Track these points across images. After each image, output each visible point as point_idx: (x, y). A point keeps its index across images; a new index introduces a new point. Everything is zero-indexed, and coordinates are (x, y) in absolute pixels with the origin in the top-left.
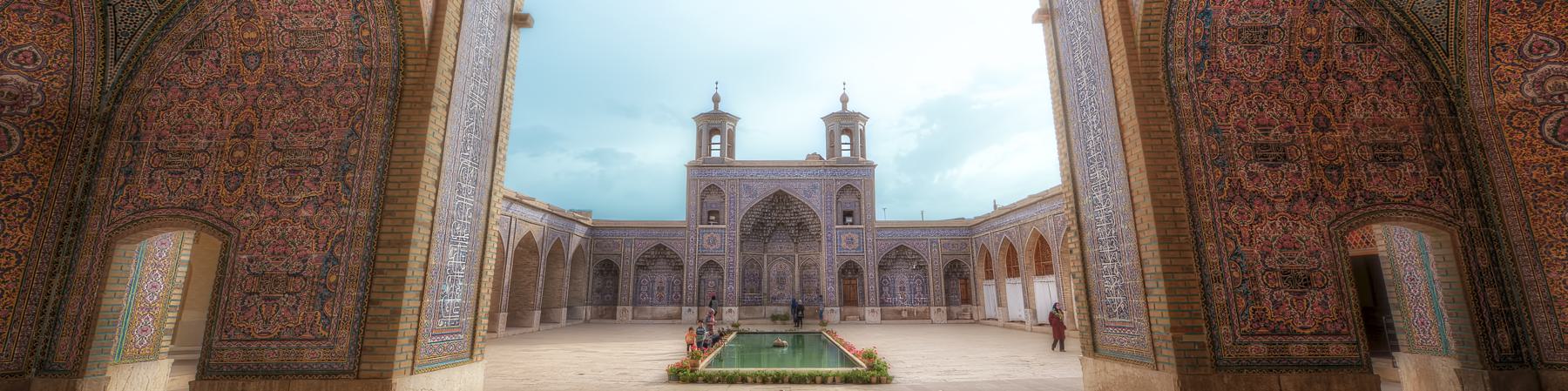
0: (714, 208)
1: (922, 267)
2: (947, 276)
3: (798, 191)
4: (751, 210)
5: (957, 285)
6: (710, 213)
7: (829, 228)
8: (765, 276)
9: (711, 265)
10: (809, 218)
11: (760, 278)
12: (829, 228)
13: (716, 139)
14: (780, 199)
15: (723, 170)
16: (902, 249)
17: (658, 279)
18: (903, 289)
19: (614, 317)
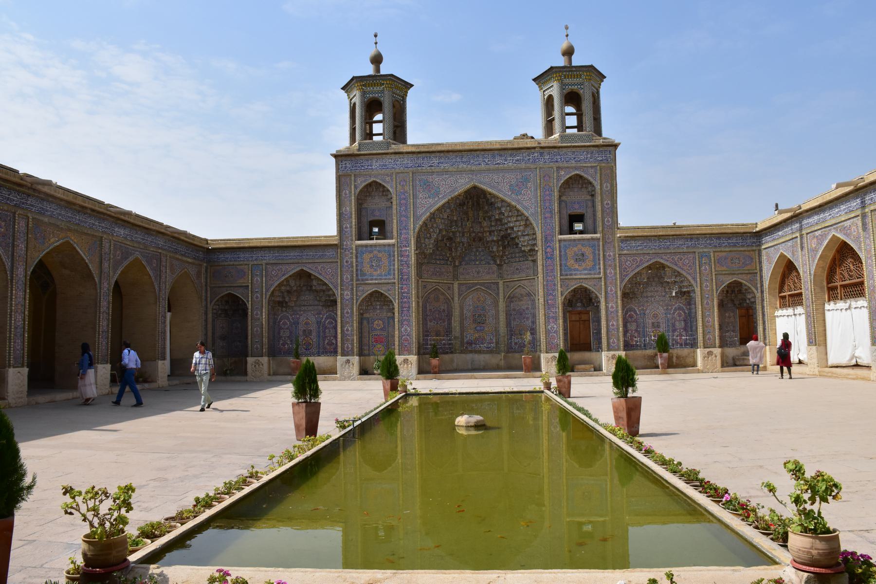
0: (377, 216)
1: (686, 295)
2: (721, 305)
3: (498, 186)
4: (433, 216)
5: (735, 317)
6: (373, 224)
7: (547, 240)
8: (456, 313)
9: (377, 299)
10: (518, 227)
11: (449, 316)
12: (547, 240)
13: (379, 117)
14: (476, 200)
15: (388, 161)
16: (661, 262)
17: (302, 319)
18: (656, 326)
19: (245, 373)
